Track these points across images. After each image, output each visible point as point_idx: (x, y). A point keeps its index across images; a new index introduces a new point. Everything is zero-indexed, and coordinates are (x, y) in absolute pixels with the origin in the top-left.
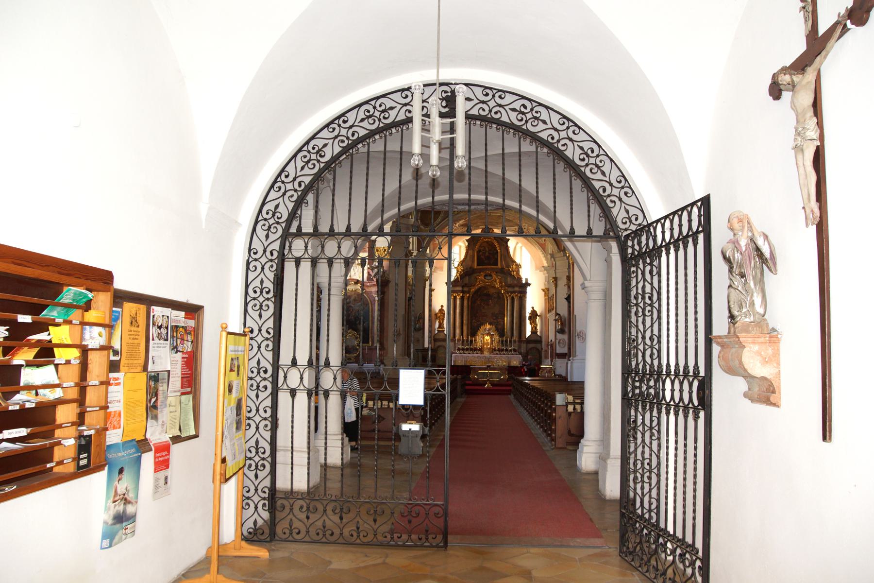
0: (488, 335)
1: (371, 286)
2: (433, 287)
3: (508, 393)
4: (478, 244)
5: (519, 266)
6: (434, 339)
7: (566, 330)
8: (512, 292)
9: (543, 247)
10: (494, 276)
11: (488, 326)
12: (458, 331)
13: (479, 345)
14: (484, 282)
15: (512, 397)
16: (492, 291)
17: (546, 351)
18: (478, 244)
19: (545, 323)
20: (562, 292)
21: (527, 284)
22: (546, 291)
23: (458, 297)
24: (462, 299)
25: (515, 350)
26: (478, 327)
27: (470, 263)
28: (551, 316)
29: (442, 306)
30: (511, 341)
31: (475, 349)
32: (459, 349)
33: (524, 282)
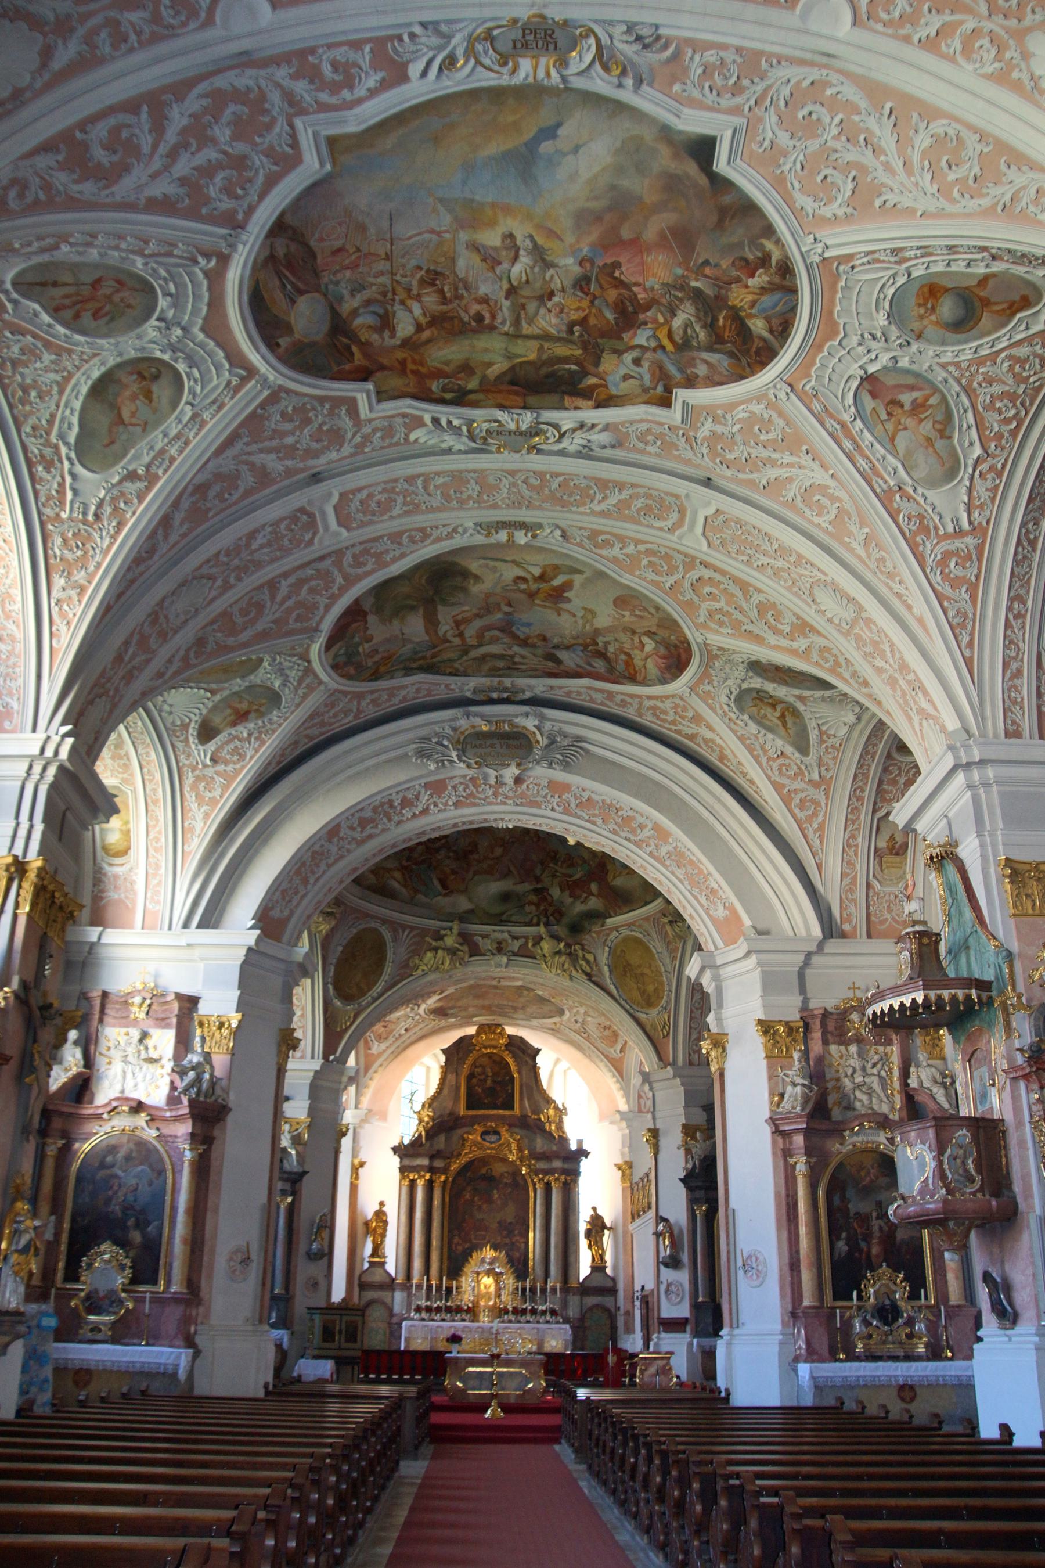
0: (489, 1272)
1: (177, 1119)
2: (363, 1156)
3: (551, 1436)
4: (470, 1059)
5: (561, 1112)
6: (357, 1280)
7: (685, 1258)
8: (546, 1172)
9: (617, 1067)
10: (505, 1135)
11: (489, 1253)
12: (417, 1264)
13: (467, 1298)
14: (481, 1148)
15: (564, 1451)
16: (499, 1169)
17: (629, 1314)
18: (470, 1059)
19: (626, 1245)
20: (675, 1163)
21: (582, 1153)
22: (626, 1169)
23: (420, 1183)
24: (430, 1186)
25: (553, 1312)
26: (466, 1256)
27: (449, 1104)
28: (644, 1230)
29: (382, 1204)
30: (543, 1290)
31: (459, 1310)
32: (418, 1309)
33: (573, 1147)
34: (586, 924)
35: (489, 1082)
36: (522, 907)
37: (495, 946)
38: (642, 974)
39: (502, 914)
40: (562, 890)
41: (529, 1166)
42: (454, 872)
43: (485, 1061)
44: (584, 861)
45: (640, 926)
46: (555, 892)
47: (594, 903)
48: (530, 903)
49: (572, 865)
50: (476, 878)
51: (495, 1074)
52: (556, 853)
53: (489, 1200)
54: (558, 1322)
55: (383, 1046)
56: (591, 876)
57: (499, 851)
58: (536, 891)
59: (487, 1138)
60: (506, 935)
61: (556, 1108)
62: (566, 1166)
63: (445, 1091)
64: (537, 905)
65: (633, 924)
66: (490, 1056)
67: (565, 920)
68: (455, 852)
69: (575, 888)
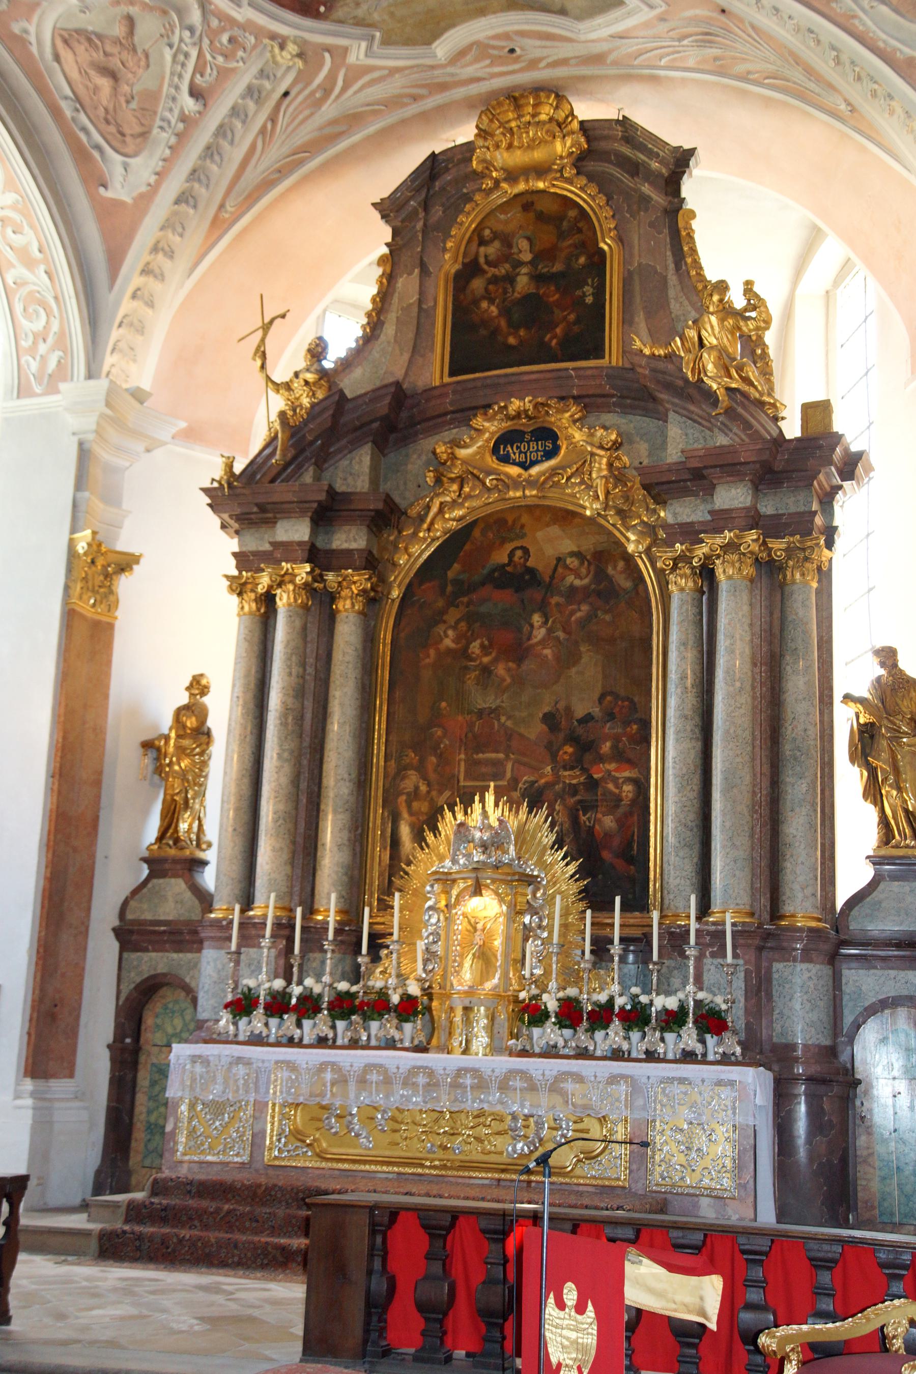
16: (550, 545)
18: (468, 221)
23: (283, 599)
24: (320, 604)
25: (711, 1022)
31: (378, 1006)
35: (523, 282)
41: (650, 530)
43: (513, 219)
51: (540, 256)
53: (518, 651)
54: (726, 1060)
55: (144, 167)
59: (513, 452)
61: (726, 311)
62: (767, 507)
63: (389, 330)
66: (527, 202)
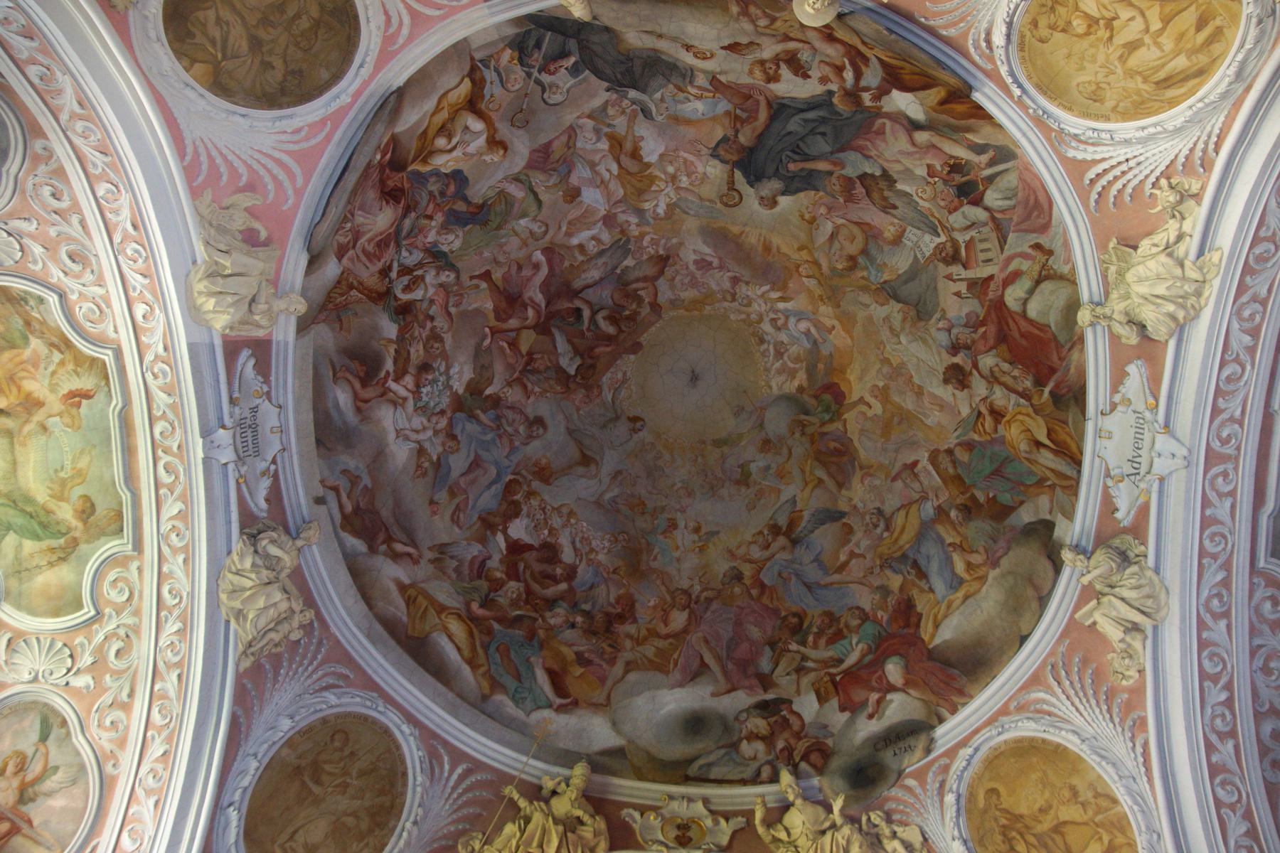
34: (887, 756)
36: (735, 746)
37: (673, 833)
38: (1058, 828)
39: (691, 761)
40: (822, 699)
42: (581, 660)
44: (865, 617)
45: (1021, 708)
46: (807, 706)
47: (899, 707)
48: (752, 737)
49: (838, 636)
50: (633, 676)
52: (801, 616)
56: (881, 649)
57: (679, 619)
58: (764, 708)
60: (699, 807)
64: (769, 740)
65: (1004, 711)
67: (836, 763)
68: (587, 615)
69: (848, 686)
